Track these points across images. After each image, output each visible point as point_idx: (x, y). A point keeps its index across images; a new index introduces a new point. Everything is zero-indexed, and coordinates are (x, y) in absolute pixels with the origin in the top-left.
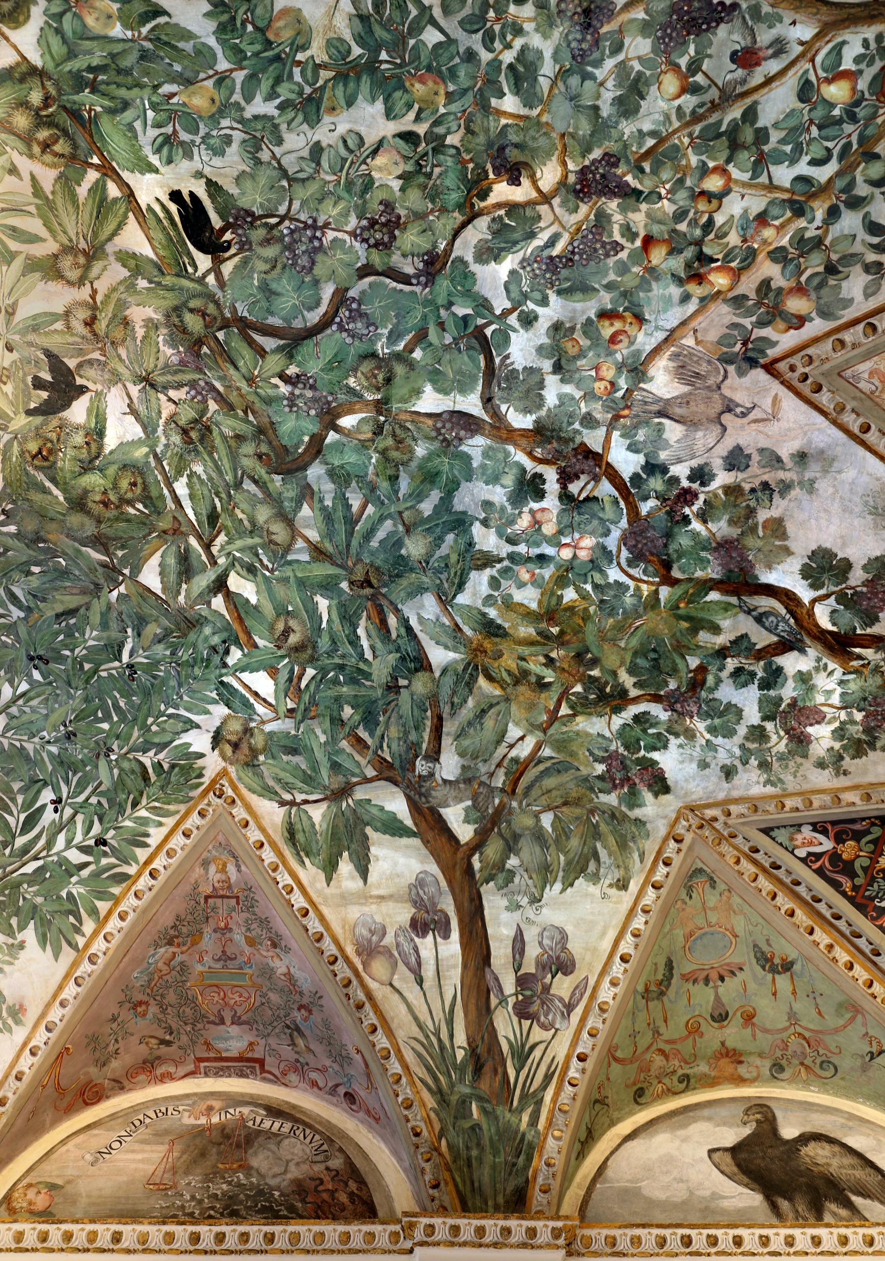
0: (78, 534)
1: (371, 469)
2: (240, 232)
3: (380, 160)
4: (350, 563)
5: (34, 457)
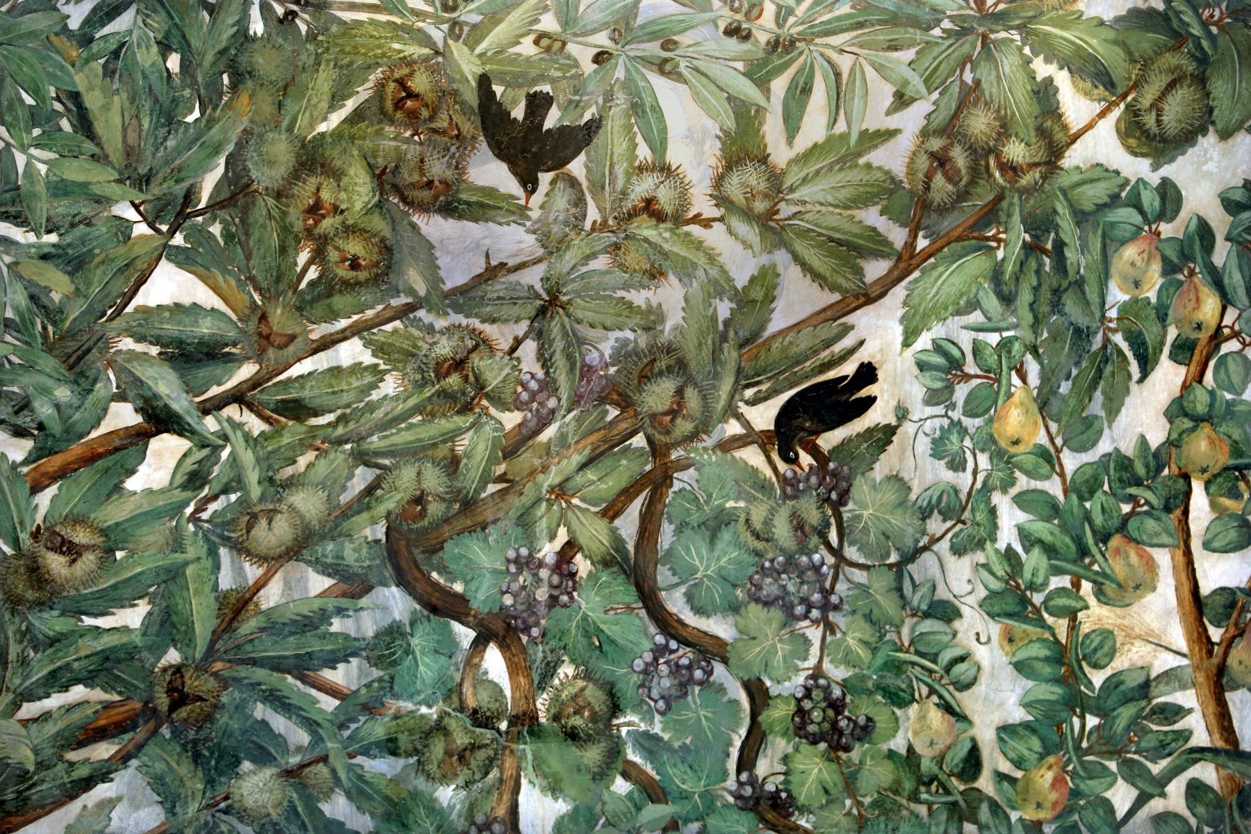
0: (251, 153)
1: (407, 705)
2: (814, 480)
3: (936, 717)
4: (218, 666)
5: (401, 83)
